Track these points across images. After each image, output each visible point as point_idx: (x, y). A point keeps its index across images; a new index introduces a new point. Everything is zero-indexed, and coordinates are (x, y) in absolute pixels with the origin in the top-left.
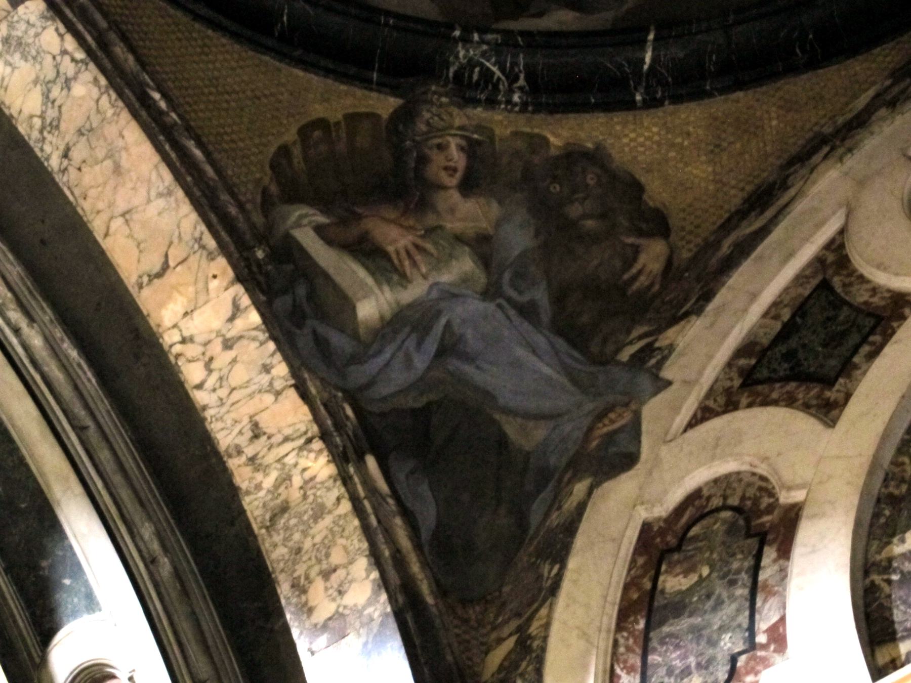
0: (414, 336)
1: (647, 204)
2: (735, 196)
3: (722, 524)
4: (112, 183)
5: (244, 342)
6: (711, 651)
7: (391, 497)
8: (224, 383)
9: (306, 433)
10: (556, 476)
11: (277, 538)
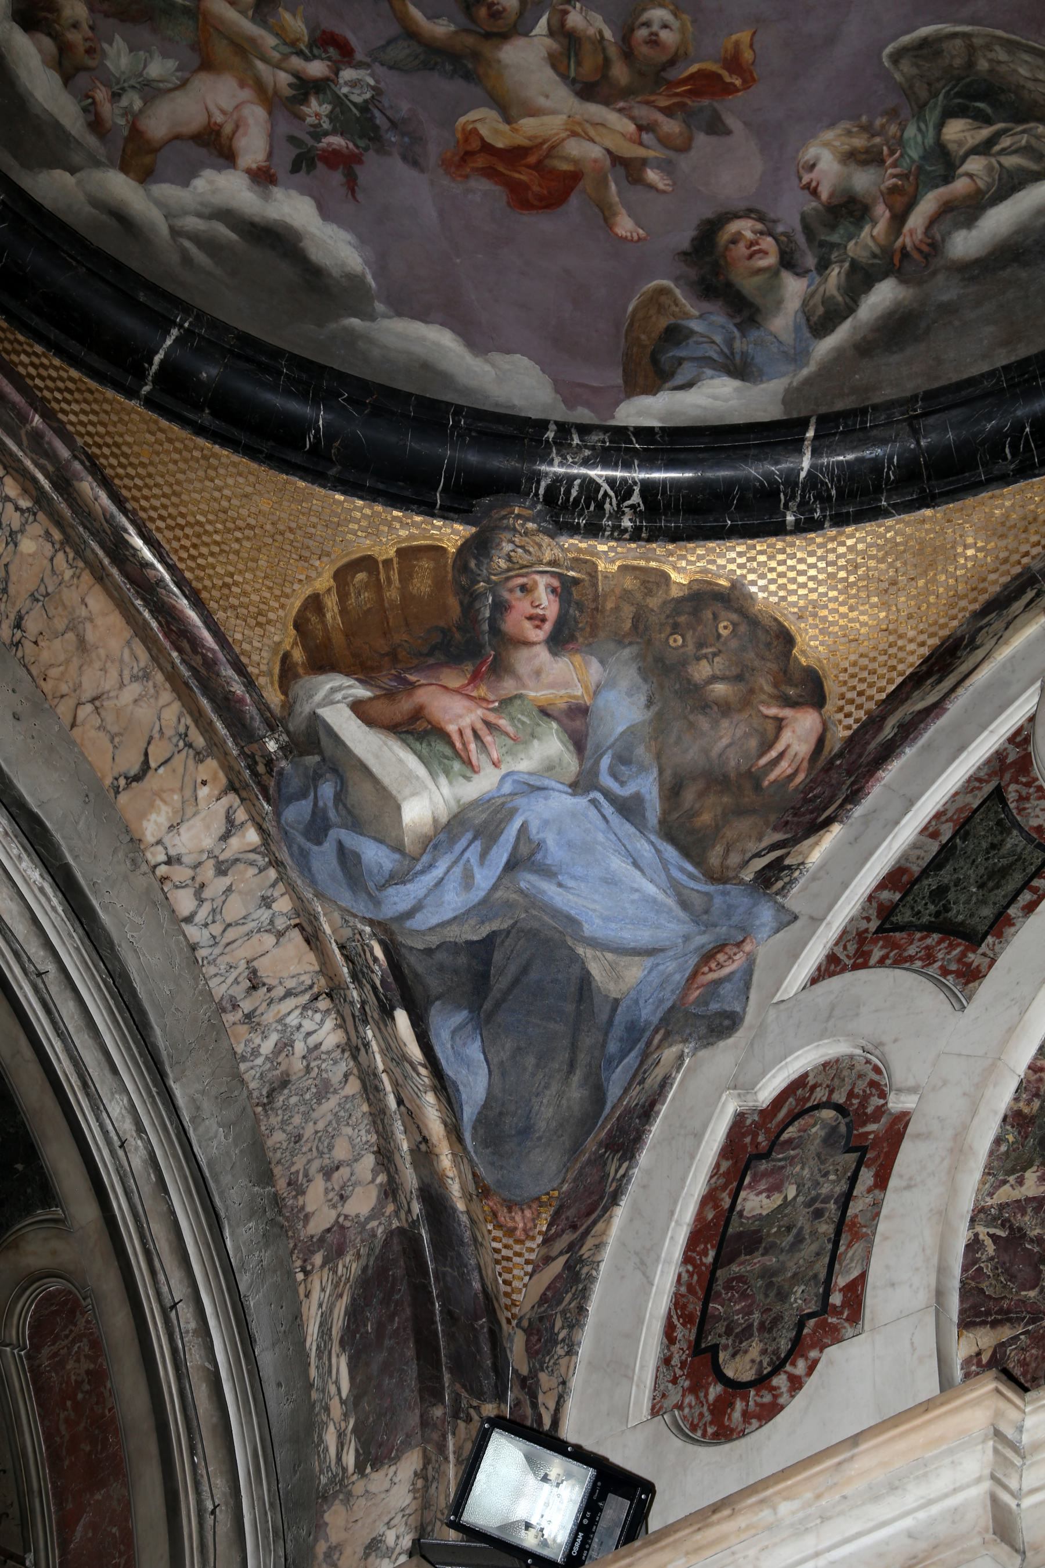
0: (477, 846)
1: (796, 659)
2: (913, 653)
3: (822, 1129)
4: (75, 662)
5: (241, 866)
6: (778, 1308)
7: (424, 1066)
8: (218, 917)
9: (311, 987)
10: (647, 1034)
11: (274, 1120)
